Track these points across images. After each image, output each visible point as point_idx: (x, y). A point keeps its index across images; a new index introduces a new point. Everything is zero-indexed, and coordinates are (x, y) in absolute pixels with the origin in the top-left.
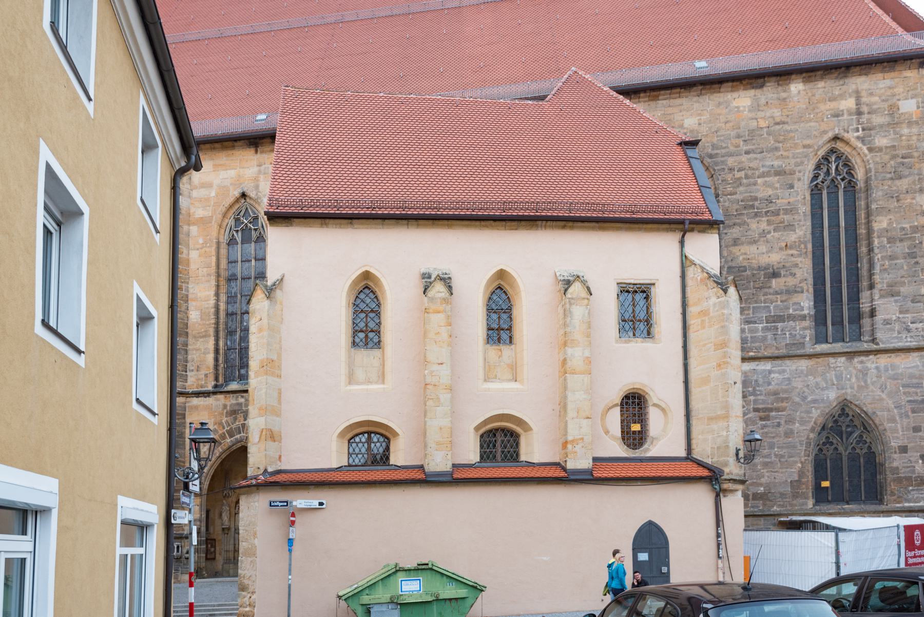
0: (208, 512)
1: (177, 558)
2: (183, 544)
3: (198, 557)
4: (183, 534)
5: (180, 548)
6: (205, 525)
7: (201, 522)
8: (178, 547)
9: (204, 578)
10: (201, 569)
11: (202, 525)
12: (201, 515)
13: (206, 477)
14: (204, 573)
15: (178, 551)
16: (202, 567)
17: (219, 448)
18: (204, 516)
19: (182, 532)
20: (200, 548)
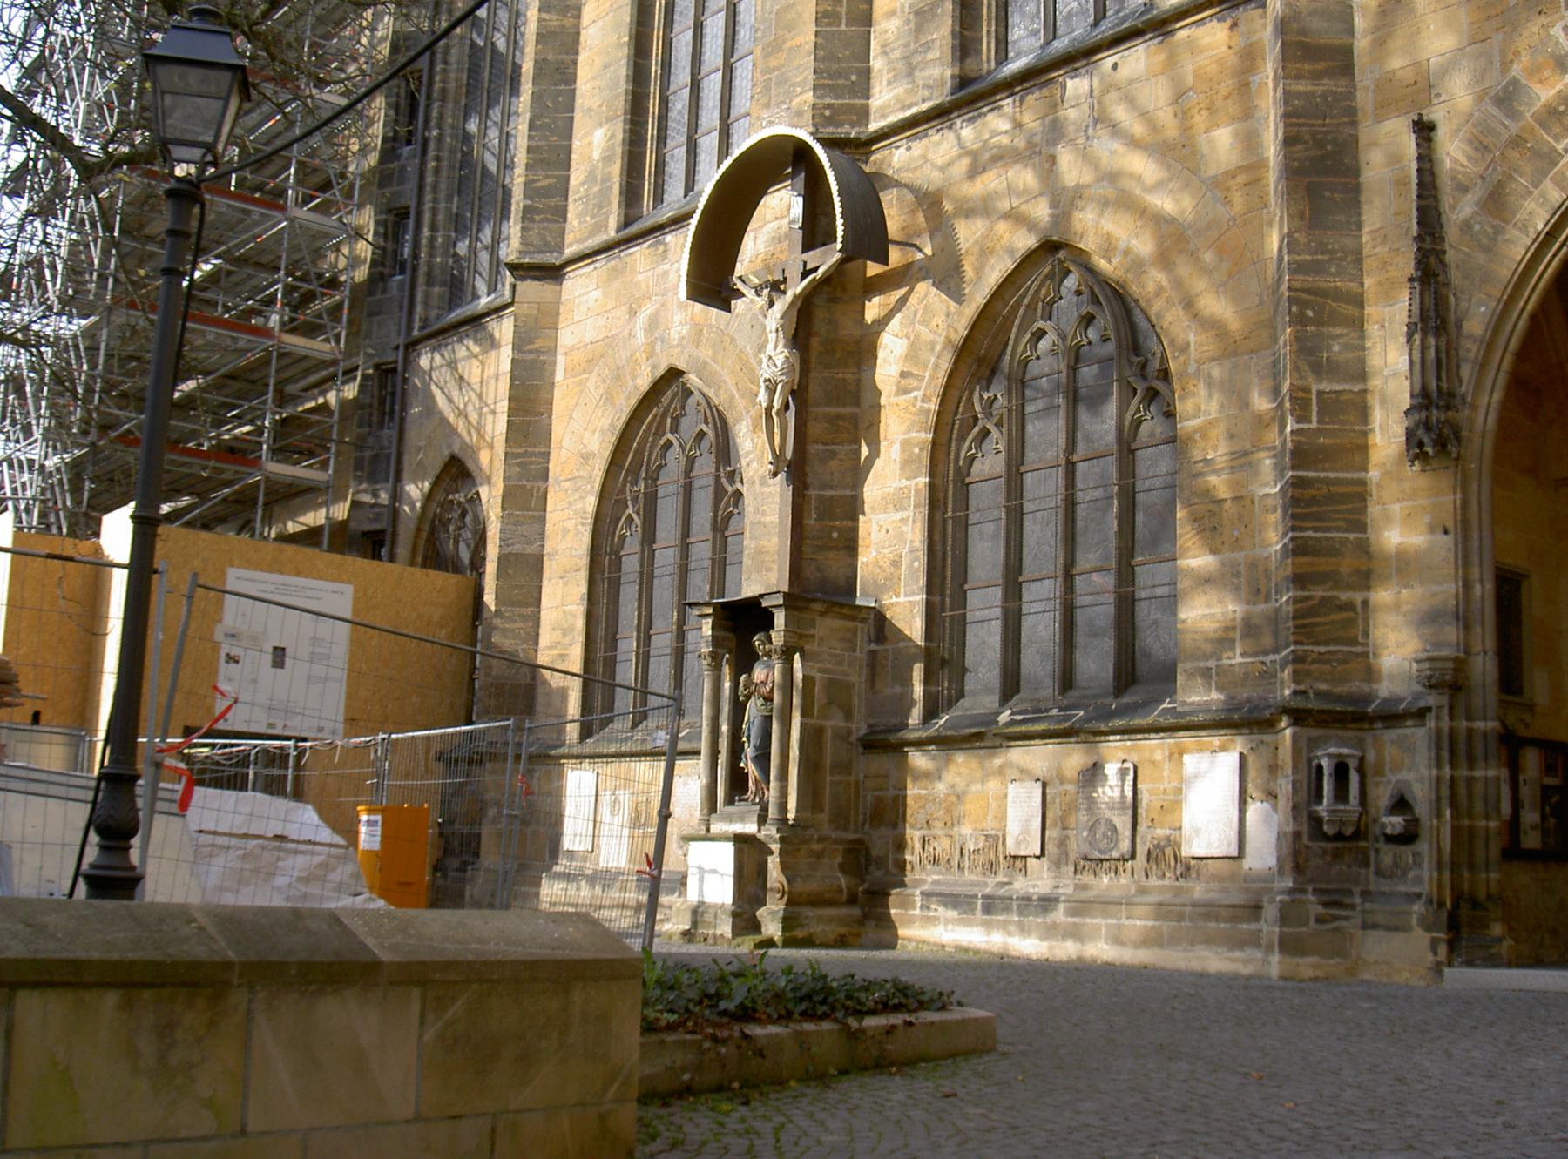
0: (1508, 587)
1: (1339, 837)
2: (1371, 756)
3: (1456, 831)
4: (1368, 699)
5: (1354, 777)
6: (1491, 643)
7: (1467, 627)
8: (1341, 771)
9: (1493, 962)
10: (1475, 904)
11: (1477, 647)
12: (1467, 585)
13: (1483, 365)
14: (1497, 929)
15: (1341, 793)
16: (1481, 895)
17: (1547, 184)
18: (1483, 590)
19: (1366, 688)
20: (1470, 781)
